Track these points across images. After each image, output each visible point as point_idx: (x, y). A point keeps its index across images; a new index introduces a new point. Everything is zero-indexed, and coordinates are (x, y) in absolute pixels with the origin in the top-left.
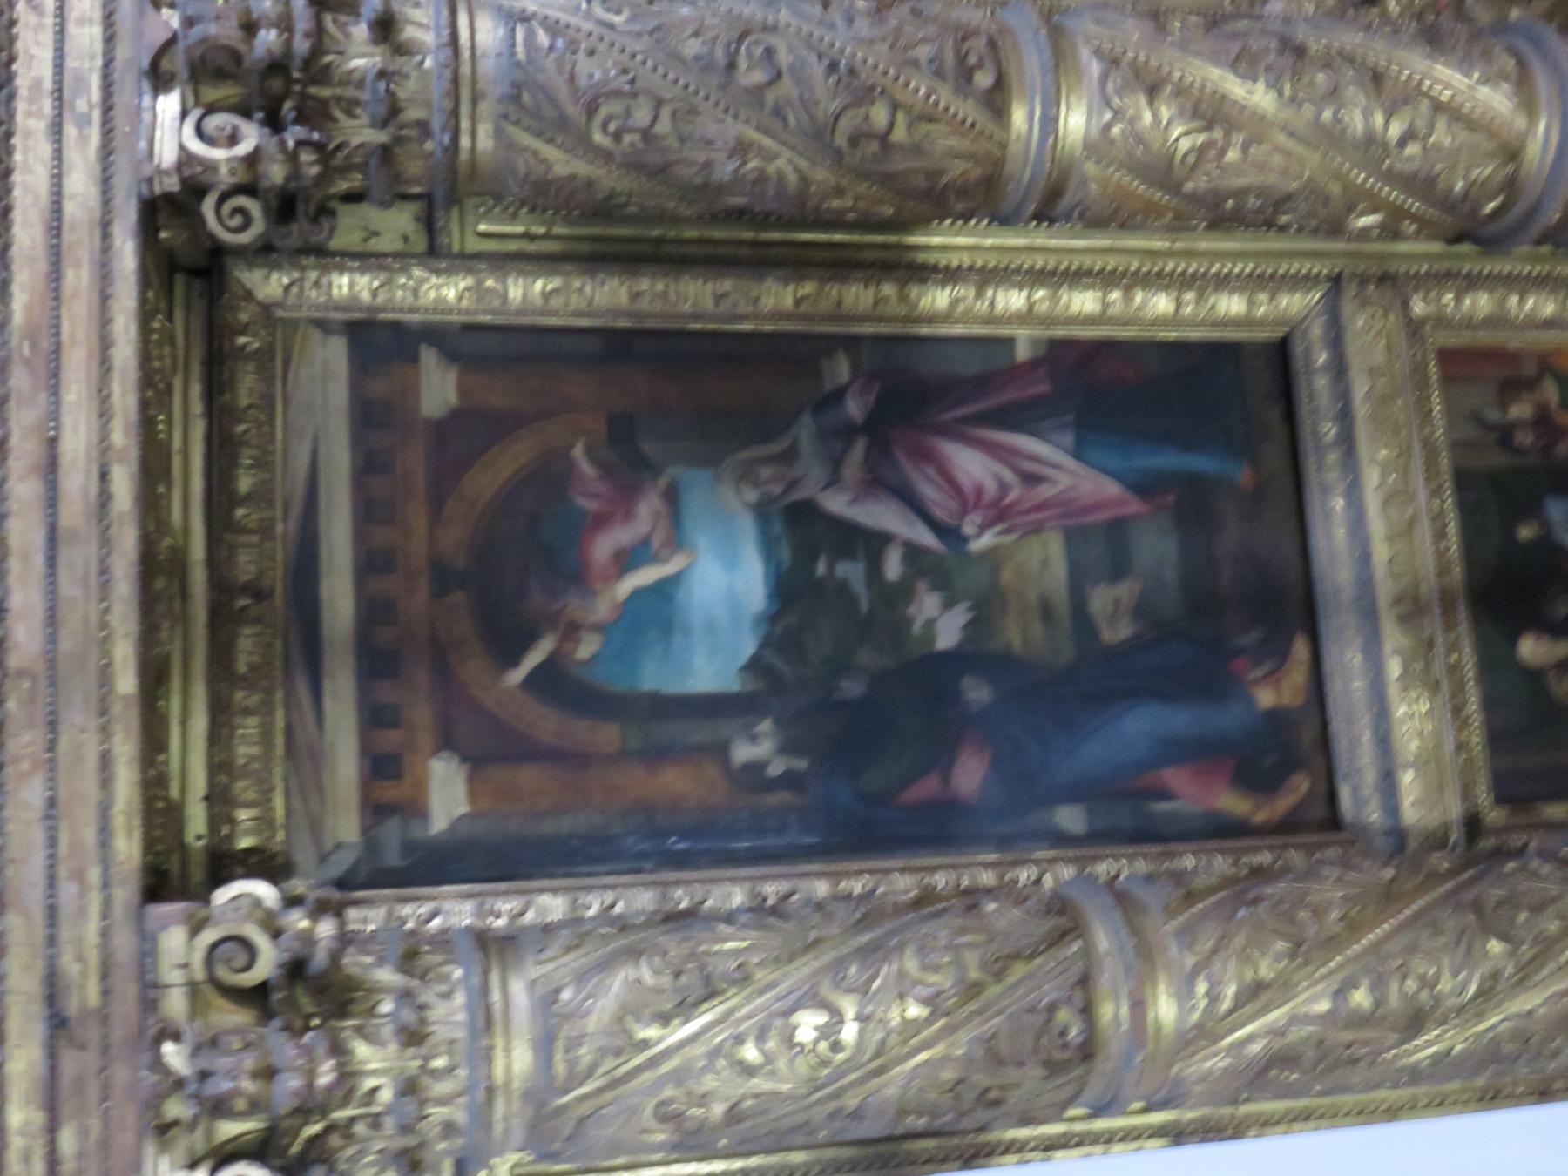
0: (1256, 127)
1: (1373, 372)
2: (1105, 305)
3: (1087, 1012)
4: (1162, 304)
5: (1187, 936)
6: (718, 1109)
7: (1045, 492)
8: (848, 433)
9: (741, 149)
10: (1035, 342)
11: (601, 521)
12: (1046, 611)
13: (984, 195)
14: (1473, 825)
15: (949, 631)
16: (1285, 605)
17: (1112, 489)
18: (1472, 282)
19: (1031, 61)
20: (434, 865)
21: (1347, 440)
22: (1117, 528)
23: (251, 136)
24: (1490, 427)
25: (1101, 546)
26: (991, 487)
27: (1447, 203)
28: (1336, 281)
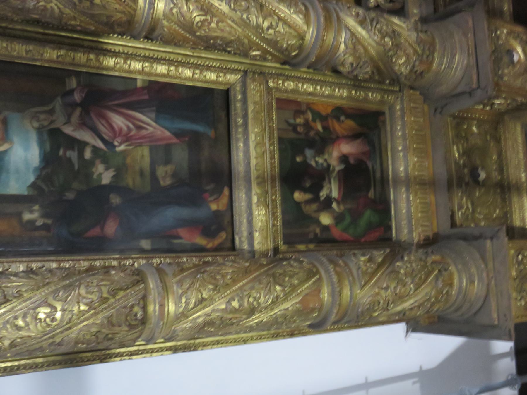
0: (222, 17)
1: (255, 103)
2: (169, 71)
3: (144, 308)
4: (188, 73)
5: (180, 283)
6: (7, 343)
7: (144, 132)
8: (74, 105)
10: (144, 81)
12: (142, 173)
14: (276, 250)
15: (107, 178)
16: (223, 177)
17: (168, 134)
18: (288, 78)
21: (245, 124)
22: (168, 148)
25: (162, 152)
26: (125, 128)
27: (281, 51)
28: (246, 72)
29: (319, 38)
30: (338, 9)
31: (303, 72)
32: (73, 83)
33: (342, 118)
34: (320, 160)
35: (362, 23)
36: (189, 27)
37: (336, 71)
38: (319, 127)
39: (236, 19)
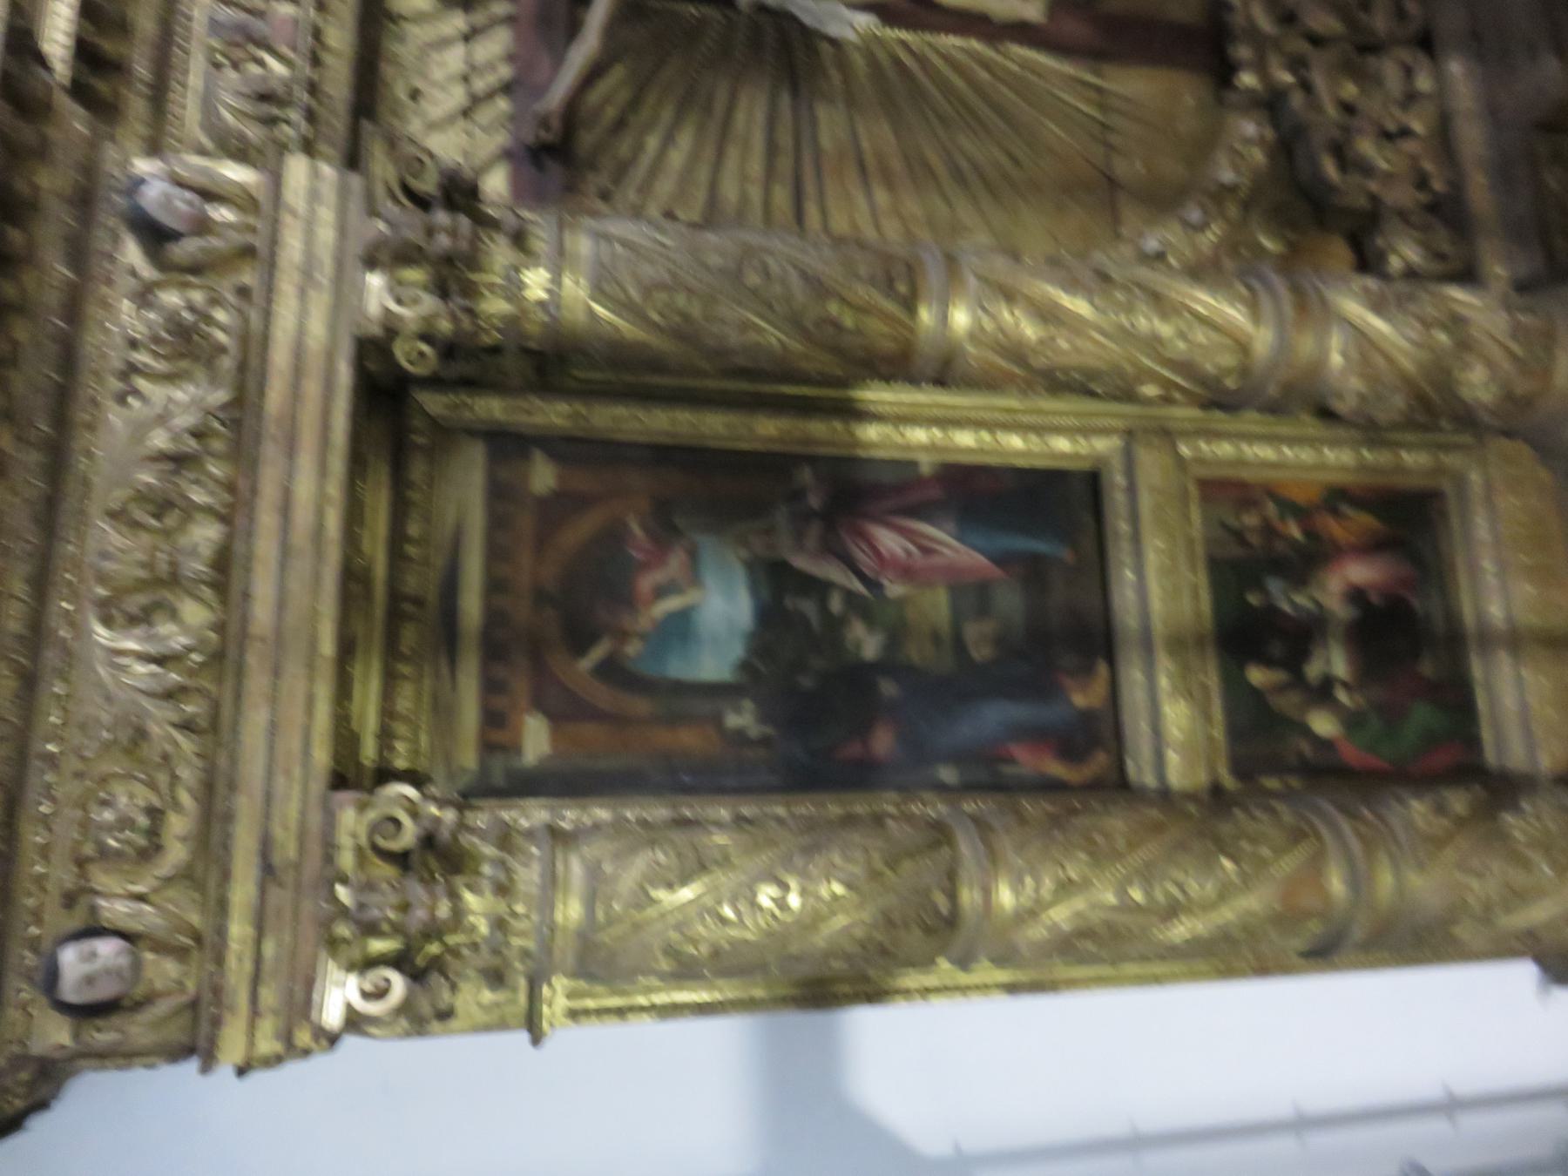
3: (953, 896)
4: (1015, 442)
5: (1020, 848)
6: (704, 949)
7: (936, 560)
9: (745, 326)
11: (645, 566)
12: (936, 637)
13: (899, 365)
14: (1216, 790)
16: (1095, 640)
17: (981, 560)
19: (933, 275)
20: (526, 785)
23: (429, 303)
25: (972, 596)
30: (1321, 286)
31: (1251, 420)
32: (806, 476)
34: (1300, 600)
35: (1378, 307)
36: (1016, 352)
37: (1326, 414)
38: (1295, 531)
39: (1105, 325)
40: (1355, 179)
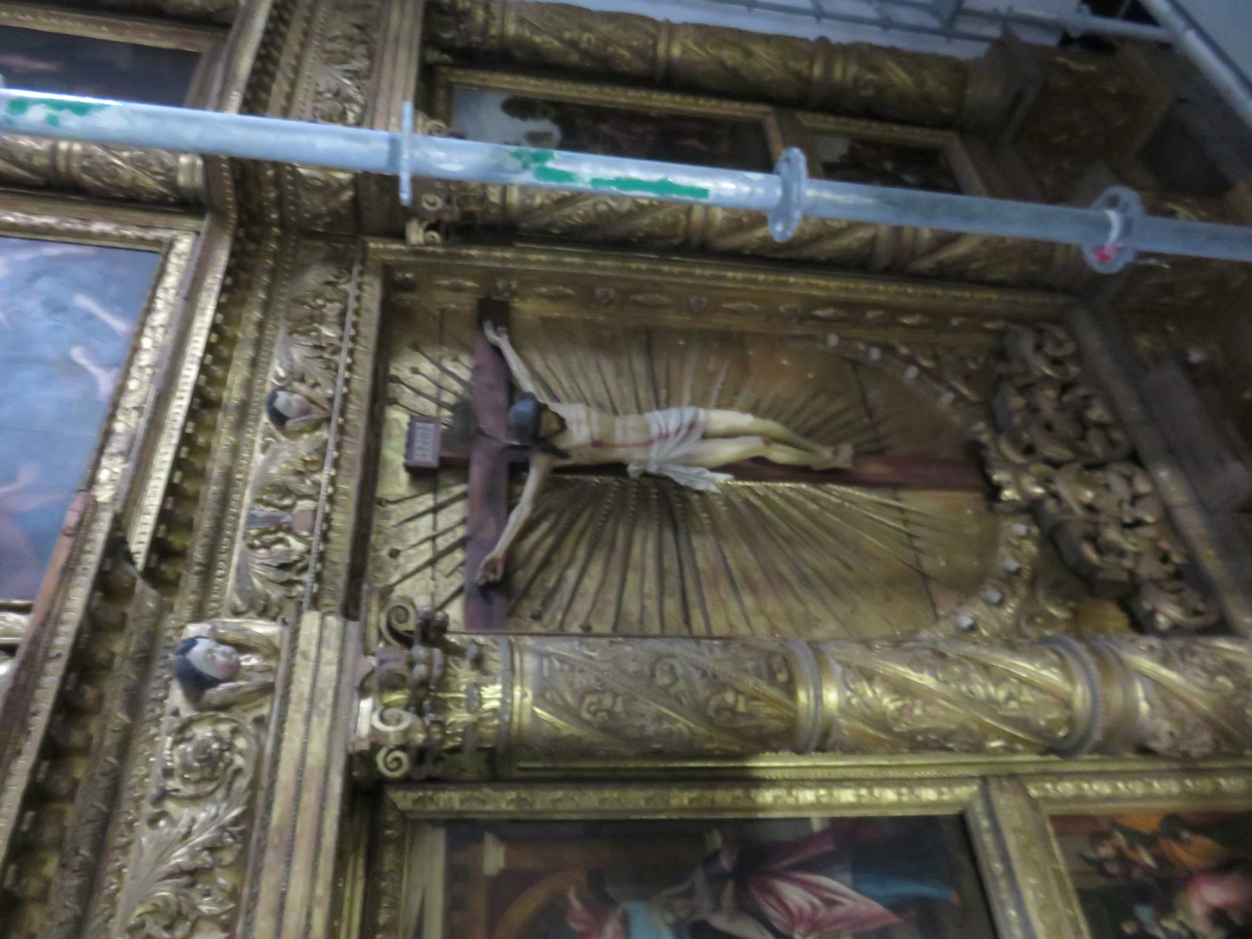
0: (926, 696)
1: (1016, 831)
2: (859, 796)
4: (890, 795)
7: (838, 911)
8: (722, 877)
9: (659, 718)
10: (823, 820)
13: (787, 738)
17: (878, 908)
18: (1060, 776)
19: (805, 664)
21: (1009, 872)
23: (408, 719)
24: (1089, 861)
26: (807, 908)
27: (1038, 733)
28: (984, 780)
29: (1095, 699)
30: (1114, 647)
31: (1085, 763)
32: (716, 840)
33: (1186, 835)
34: (1171, 925)
35: (1165, 661)
36: (881, 722)
37: (1144, 751)
38: (1147, 859)
39: (950, 695)
40: (1111, 559)
